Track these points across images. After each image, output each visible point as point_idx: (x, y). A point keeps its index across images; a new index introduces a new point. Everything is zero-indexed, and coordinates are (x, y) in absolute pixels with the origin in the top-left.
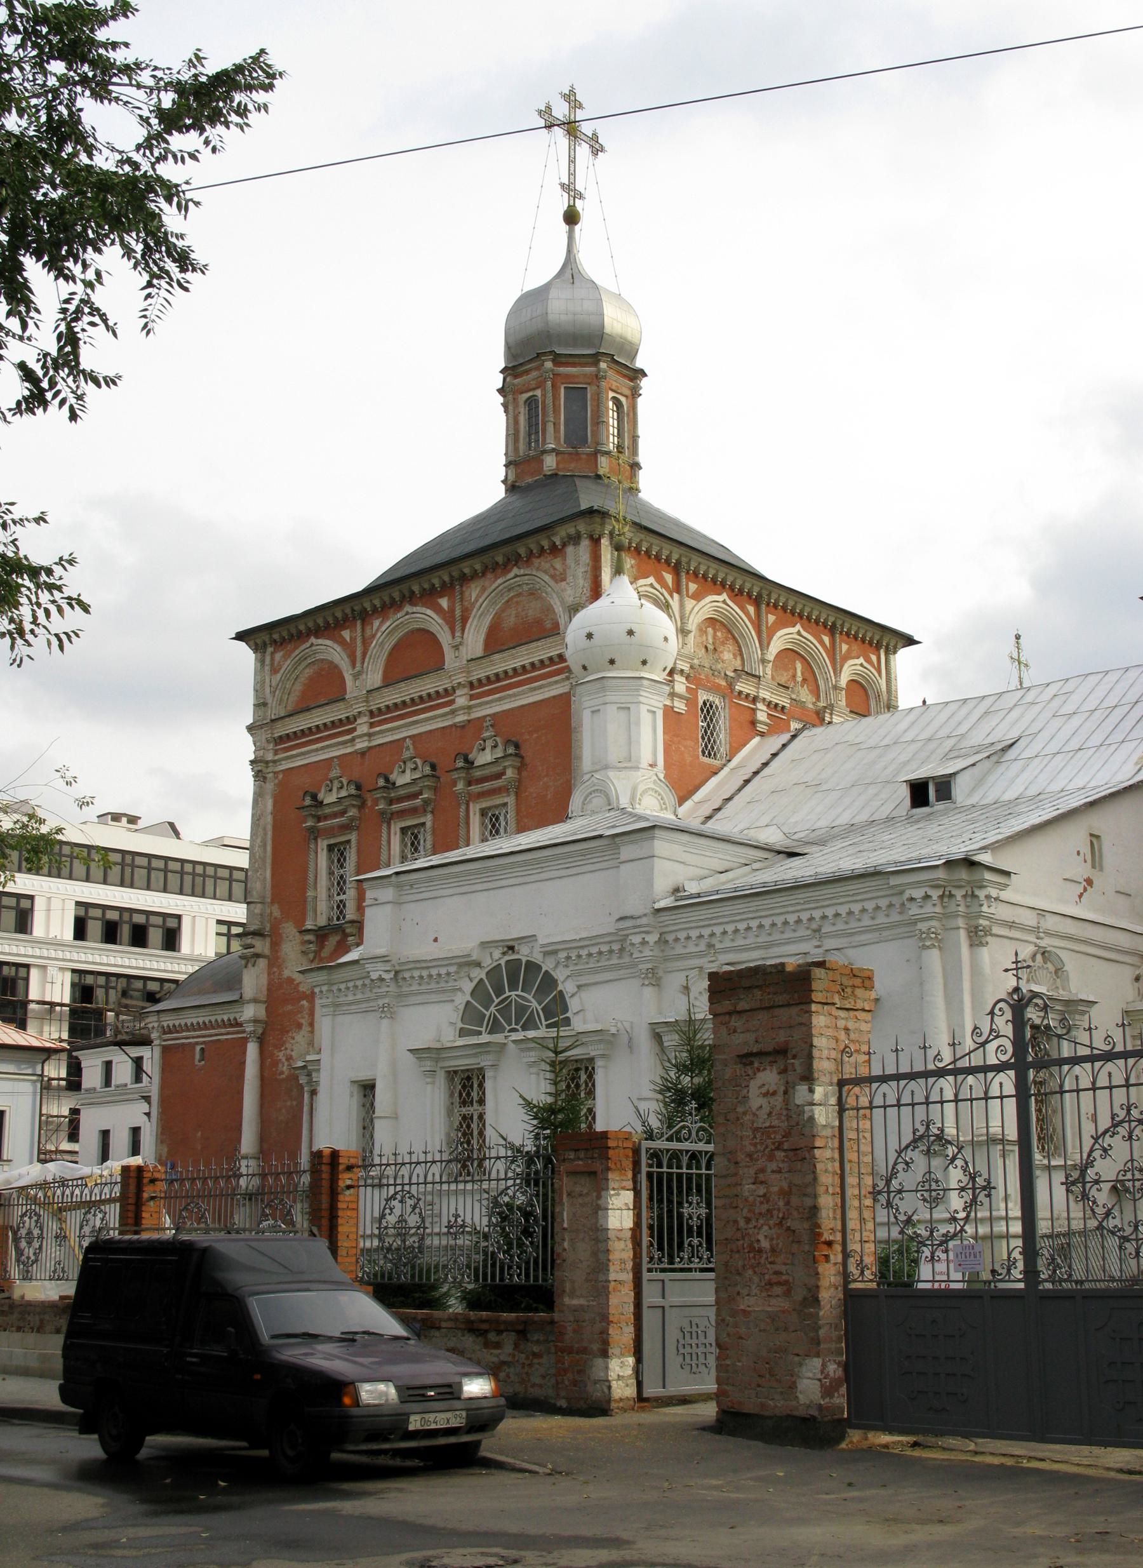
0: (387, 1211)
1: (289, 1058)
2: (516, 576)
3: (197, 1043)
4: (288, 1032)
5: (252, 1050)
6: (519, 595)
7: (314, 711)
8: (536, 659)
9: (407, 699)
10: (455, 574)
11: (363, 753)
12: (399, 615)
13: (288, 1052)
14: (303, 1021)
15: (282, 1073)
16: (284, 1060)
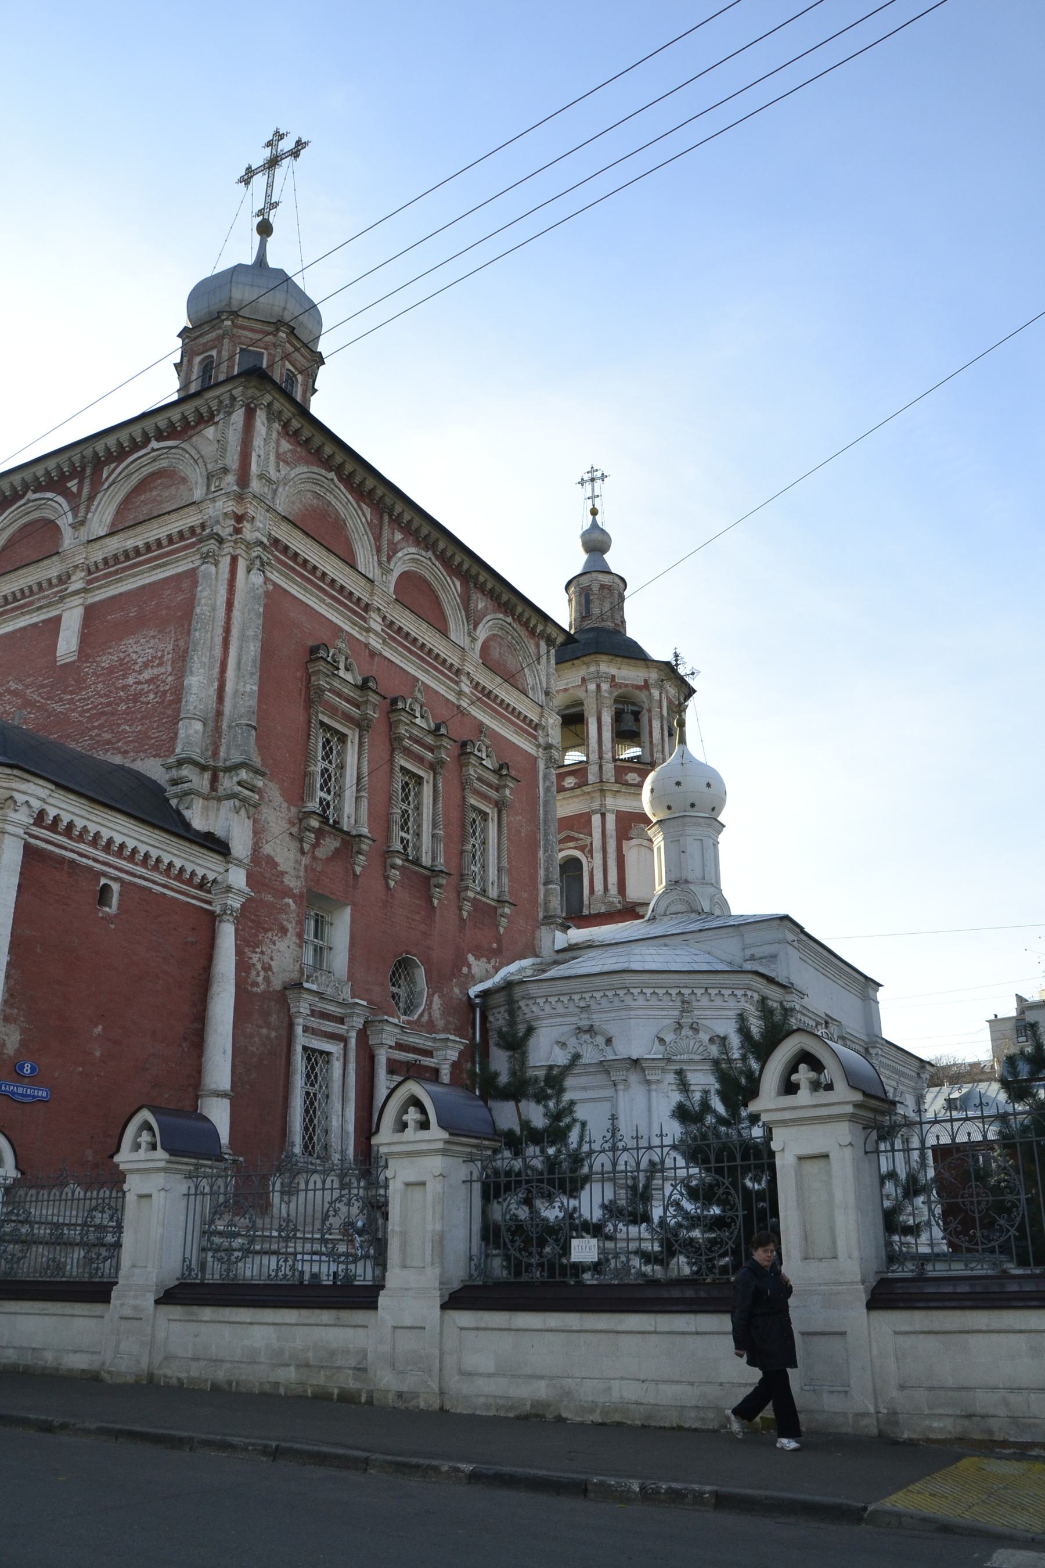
0: (331, 1213)
1: (267, 968)
2: (510, 624)
3: (105, 874)
4: (266, 930)
5: (227, 936)
6: (502, 638)
7: (332, 557)
8: (519, 709)
9: (421, 640)
10: (473, 572)
11: (373, 654)
12: (423, 553)
13: (266, 959)
14: (289, 926)
15: (256, 984)
16: (259, 967)
